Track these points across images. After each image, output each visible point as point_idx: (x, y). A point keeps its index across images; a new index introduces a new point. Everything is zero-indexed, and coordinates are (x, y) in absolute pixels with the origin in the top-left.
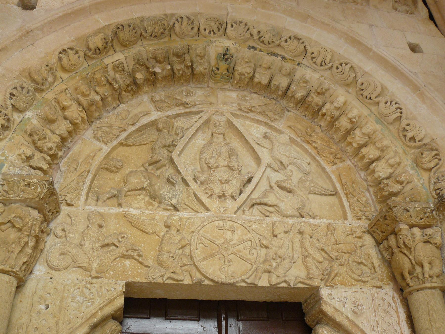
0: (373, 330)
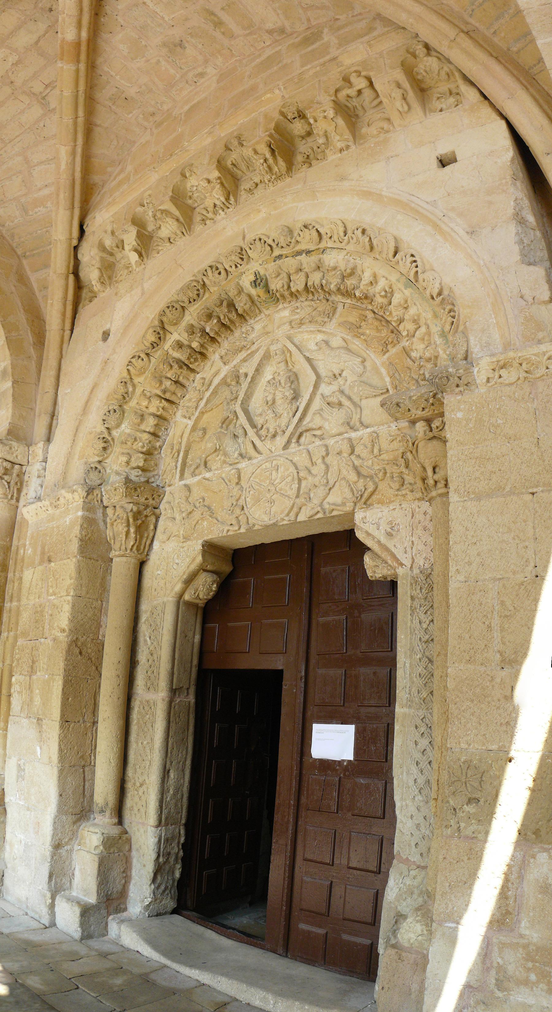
0: (405, 553)
